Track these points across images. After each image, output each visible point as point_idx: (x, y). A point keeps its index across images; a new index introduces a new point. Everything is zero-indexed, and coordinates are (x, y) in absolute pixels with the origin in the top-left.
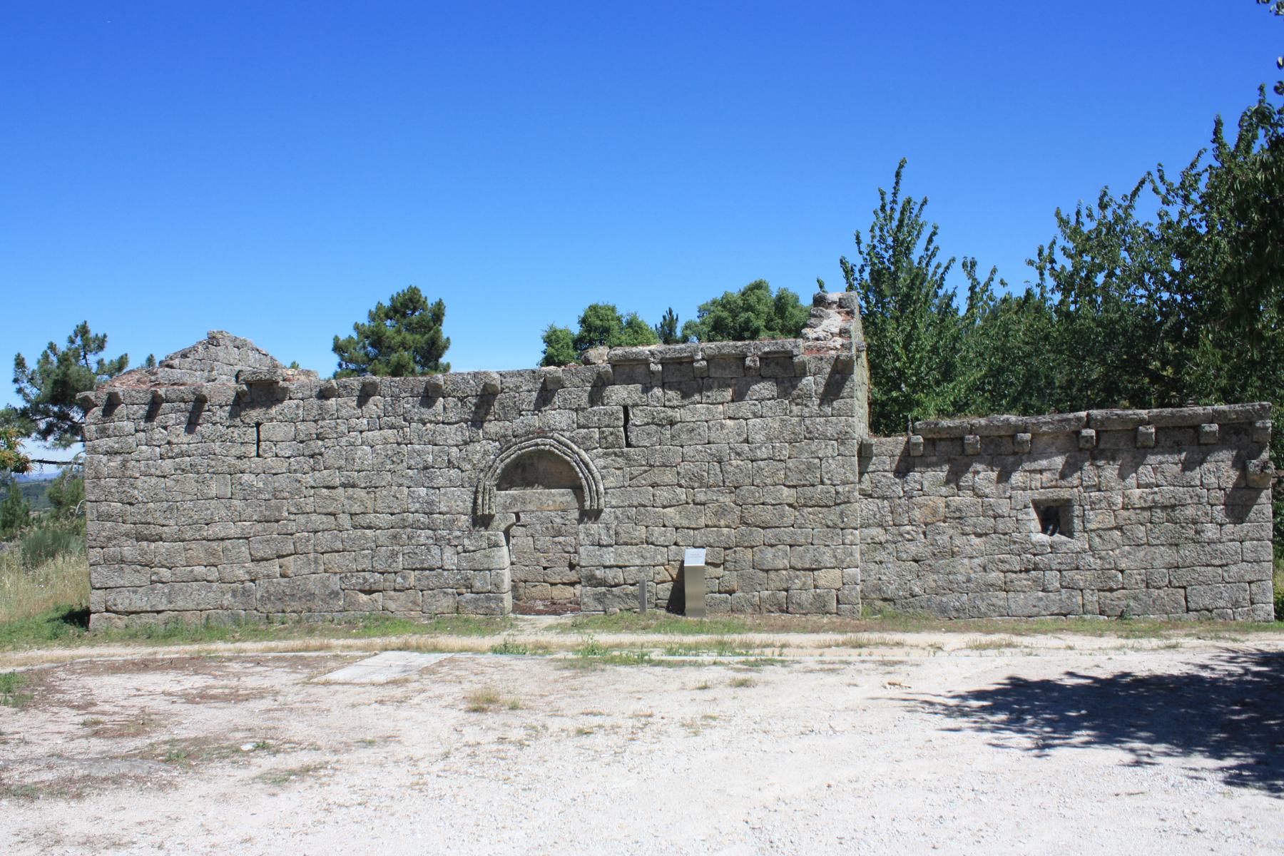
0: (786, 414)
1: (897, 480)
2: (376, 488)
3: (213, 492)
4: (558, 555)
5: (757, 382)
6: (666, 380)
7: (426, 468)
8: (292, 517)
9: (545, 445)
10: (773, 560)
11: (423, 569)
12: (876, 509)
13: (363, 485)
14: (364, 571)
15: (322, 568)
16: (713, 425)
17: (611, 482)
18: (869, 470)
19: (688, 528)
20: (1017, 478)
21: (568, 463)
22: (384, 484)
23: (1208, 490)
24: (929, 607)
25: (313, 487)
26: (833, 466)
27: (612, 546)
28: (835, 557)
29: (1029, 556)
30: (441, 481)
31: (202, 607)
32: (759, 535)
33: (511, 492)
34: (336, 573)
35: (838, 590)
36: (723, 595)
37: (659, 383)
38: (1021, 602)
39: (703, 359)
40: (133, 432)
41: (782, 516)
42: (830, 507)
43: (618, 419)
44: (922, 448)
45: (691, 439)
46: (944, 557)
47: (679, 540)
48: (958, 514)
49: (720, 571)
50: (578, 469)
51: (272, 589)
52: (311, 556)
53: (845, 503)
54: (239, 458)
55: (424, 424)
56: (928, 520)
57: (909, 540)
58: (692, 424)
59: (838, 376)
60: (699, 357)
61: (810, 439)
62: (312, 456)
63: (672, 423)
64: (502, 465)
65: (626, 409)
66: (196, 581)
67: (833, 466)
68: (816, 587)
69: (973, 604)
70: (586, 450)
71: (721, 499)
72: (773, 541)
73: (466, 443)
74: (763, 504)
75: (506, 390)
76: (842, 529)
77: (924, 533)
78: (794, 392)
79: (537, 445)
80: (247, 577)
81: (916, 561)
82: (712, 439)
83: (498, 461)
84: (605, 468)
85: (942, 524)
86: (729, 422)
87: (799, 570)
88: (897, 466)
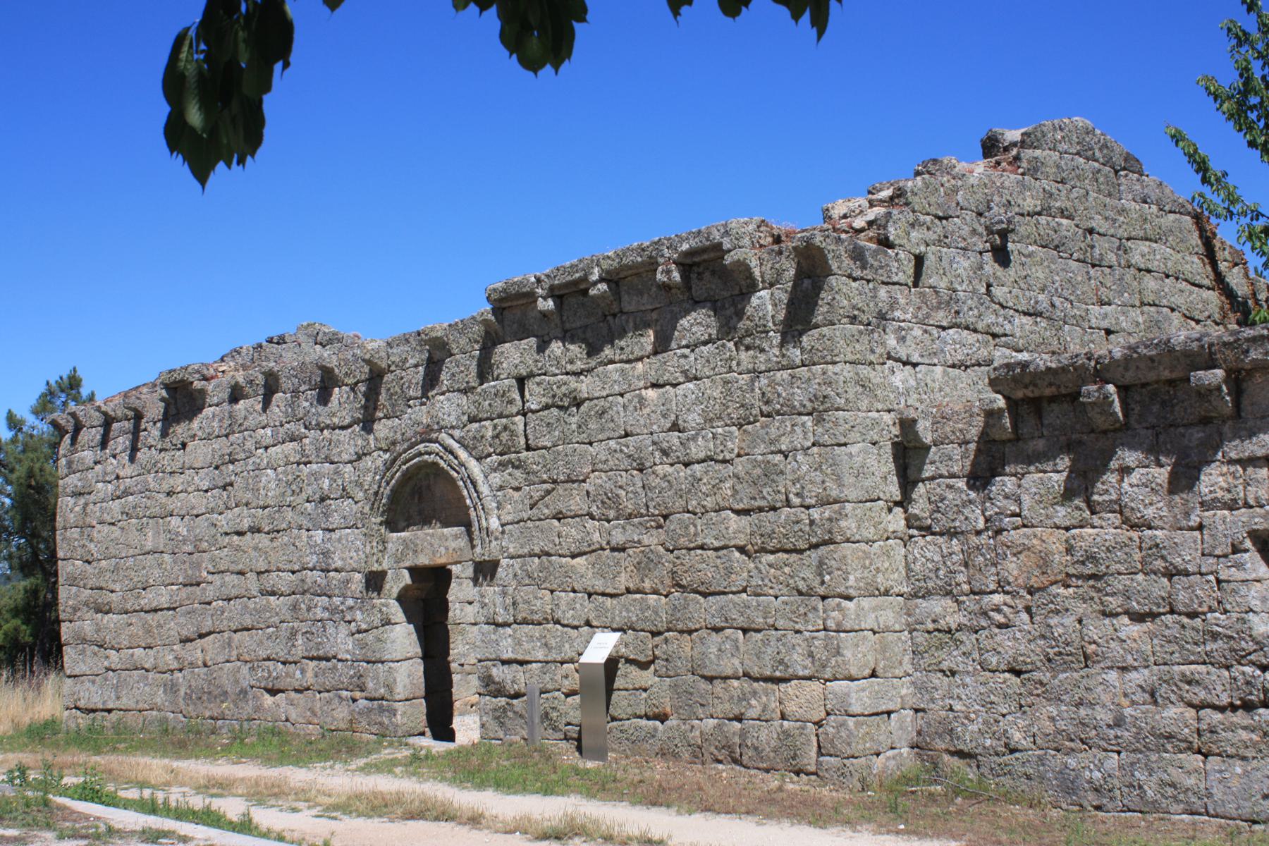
0: (731, 370)
1: (973, 495)
2: (278, 532)
3: (149, 545)
5: (687, 312)
6: (568, 326)
7: (322, 500)
8: (210, 578)
9: (430, 454)
10: (718, 657)
11: (319, 659)
12: (937, 558)
13: (267, 529)
14: (268, 659)
15: (235, 653)
16: (630, 401)
17: (509, 514)
18: (926, 474)
19: (604, 594)
20: (1213, 479)
21: (453, 481)
22: (284, 526)
24: (1042, 778)
25: (227, 534)
26: (805, 468)
27: (509, 625)
28: (811, 655)
29: (1248, 669)
30: (336, 520)
31: (140, 706)
32: (703, 610)
33: (403, 534)
34: (246, 662)
35: (818, 724)
36: (651, 723)
37: (558, 332)
38: (1235, 784)
39: (601, 280)
40: (92, 465)
41: (729, 572)
42: (801, 552)
43: (511, 402)
44: (1007, 421)
45: (602, 430)
46: (1067, 667)
47: (592, 616)
48: (1089, 569)
49: (647, 677)
50: (465, 493)
51: (193, 684)
52: (226, 635)
53: (825, 543)
54: (168, 494)
55: (322, 430)
56: (1034, 582)
57: (1000, 626)
58: (602, 402)
59: (807, 283)
60: (595, 277)
61: (769, 415)
62: (224, 488)
63: (578, 403)
64: (387, 491)
65: (521, 381)
66: (137, 669)
67: (805, 468)
68: (783, 717)
69: (1128, 779)
70: (479, 459)
71: (646, 540)
72: (718, 622)
73: (359, 458)
74: (702, 547)
75: (393, 368)
76: (824, 598)
77: (1028, 609)
78: (740, 325)
79: (420, 454)
80: (175, 665)
81: (1018, 673)
82: (629, 429)
83: (383, 484)
84: (501, 488)
85: (1061, 590)
86: (651, 394)
87: (756, 680)
88: (973, 465)
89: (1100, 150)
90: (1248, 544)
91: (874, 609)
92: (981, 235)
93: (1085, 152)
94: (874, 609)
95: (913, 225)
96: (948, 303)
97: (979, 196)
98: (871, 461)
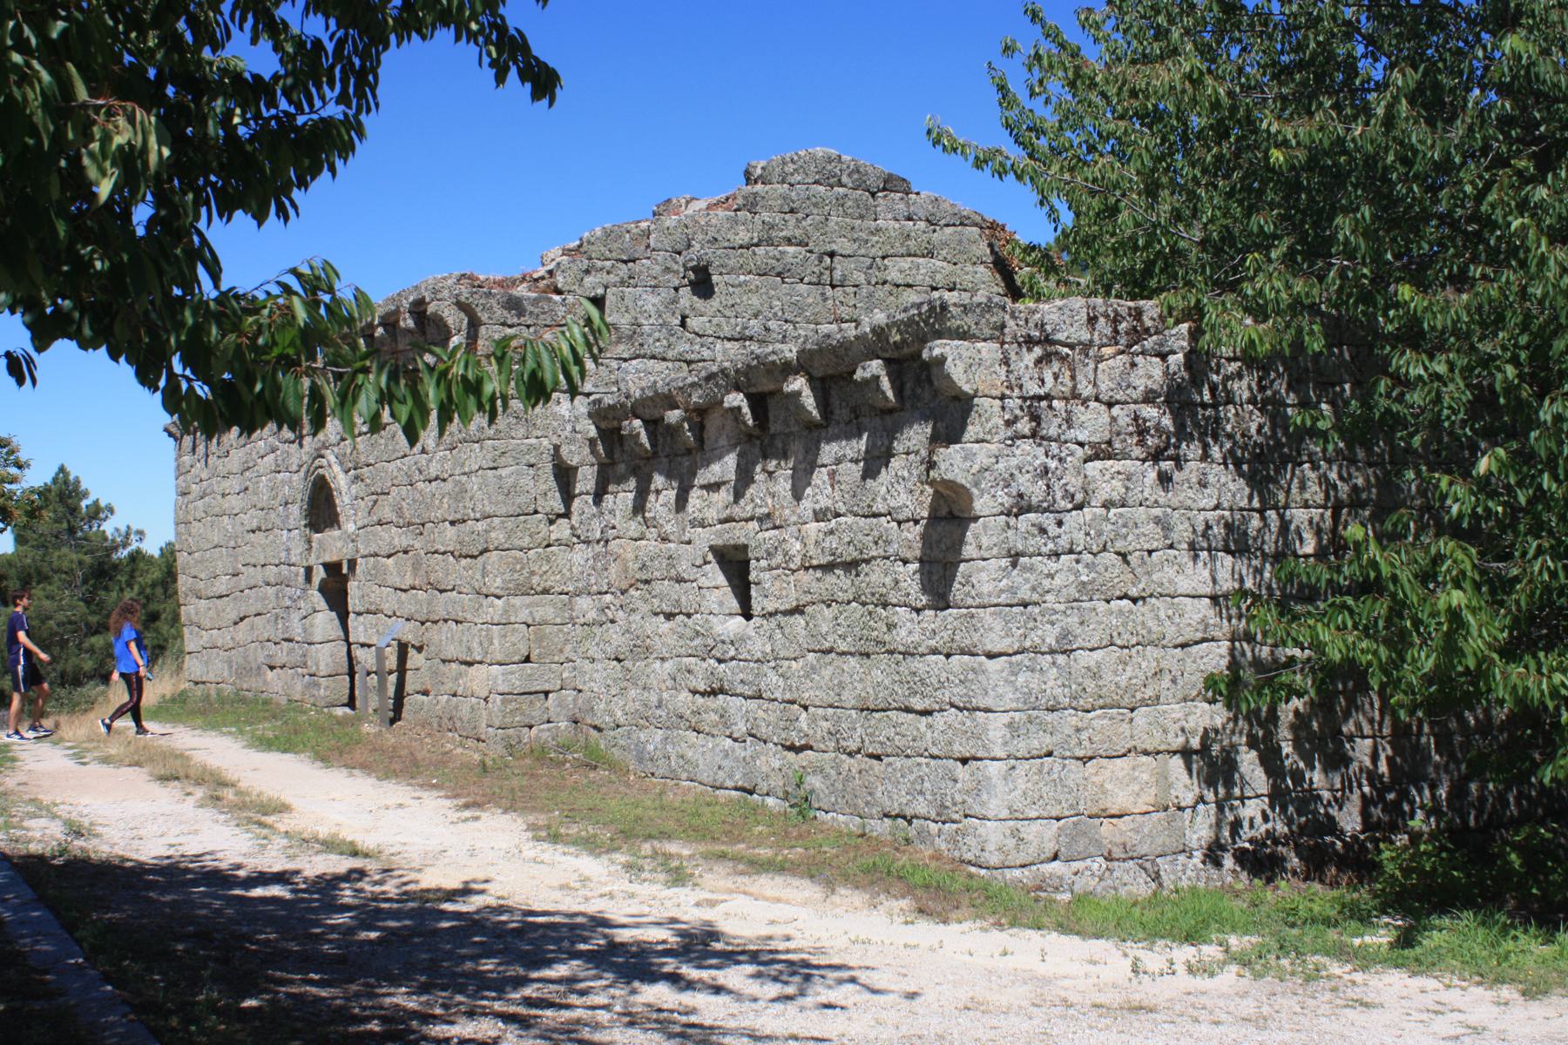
23: (899, 523)
89: (849, 175)
90: (710, 557)
91: (528, 606)
92: (677, 272)
93: (832, 181)
94: (528, 606)
95: (587, 272)
96: (631, 337)
97: (677, 236)
98: (526, 481)
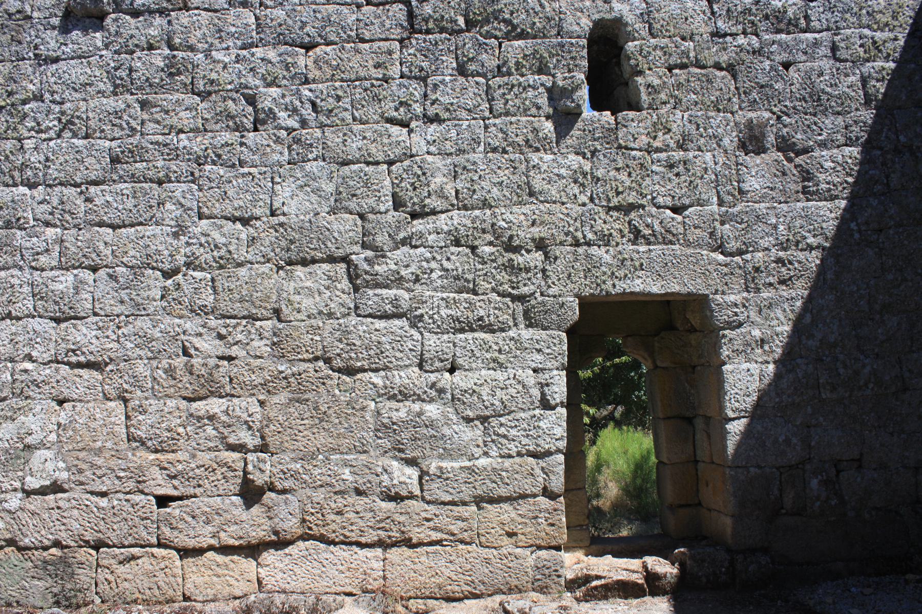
4: (205, 458)
